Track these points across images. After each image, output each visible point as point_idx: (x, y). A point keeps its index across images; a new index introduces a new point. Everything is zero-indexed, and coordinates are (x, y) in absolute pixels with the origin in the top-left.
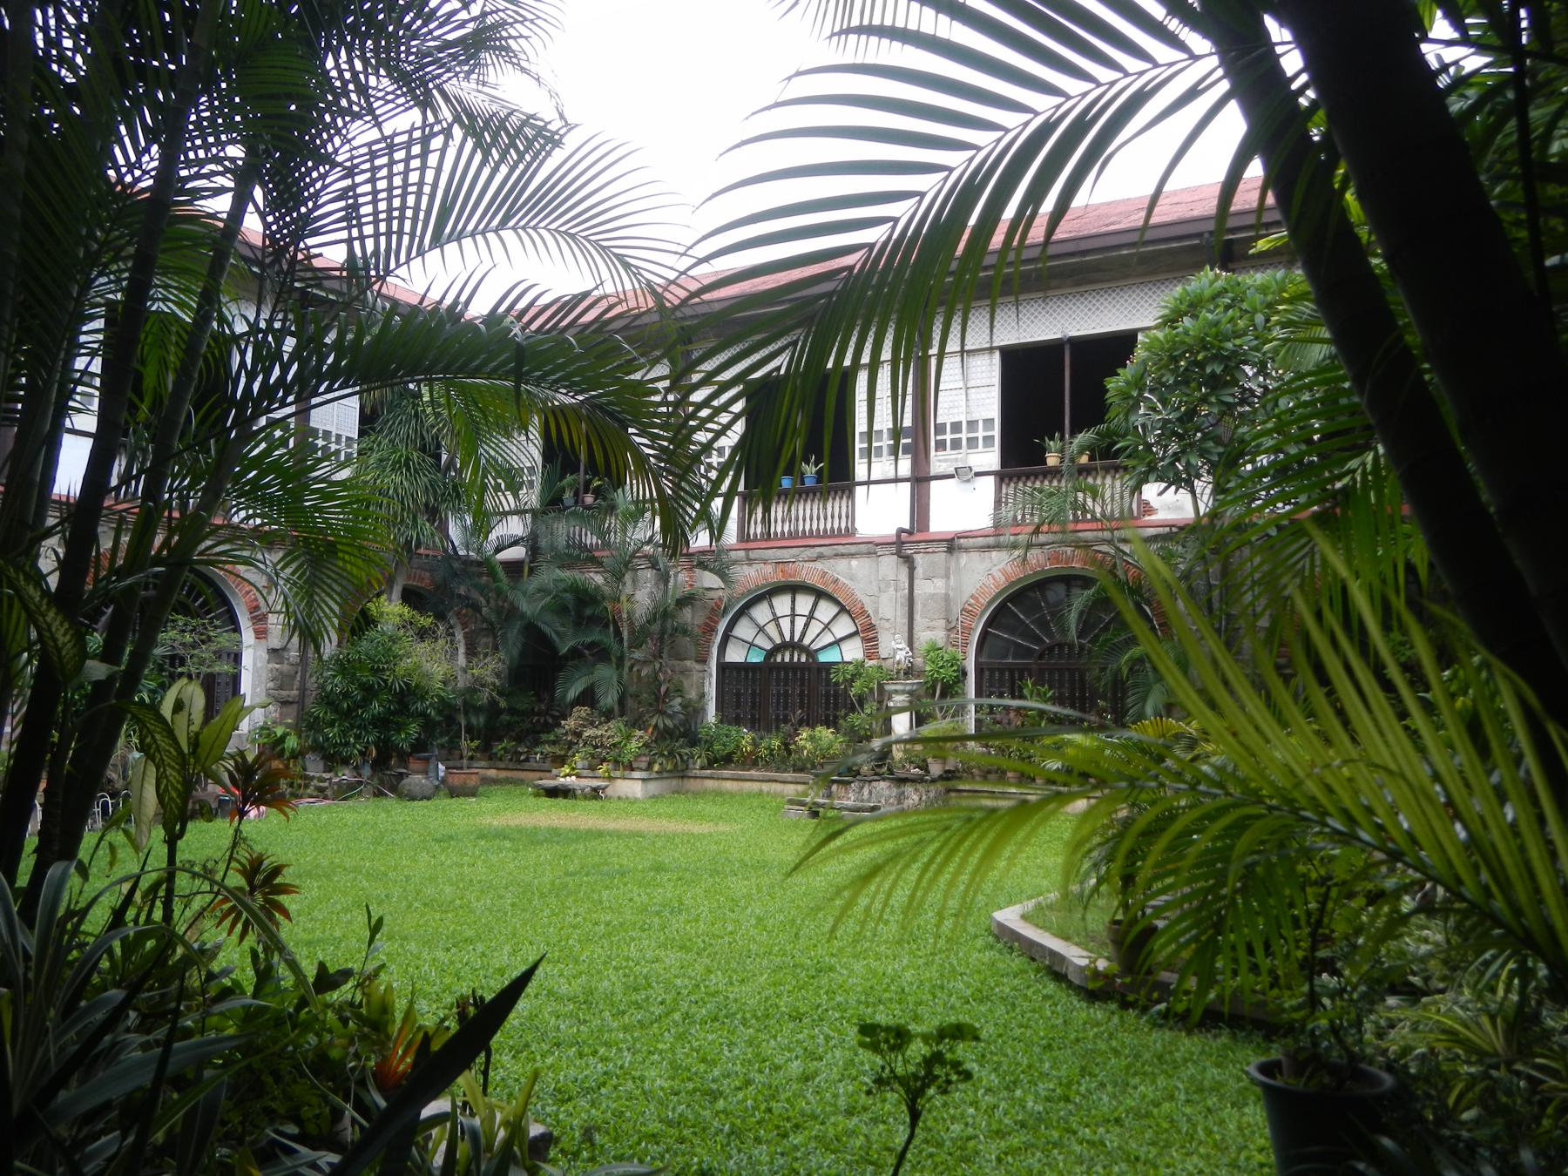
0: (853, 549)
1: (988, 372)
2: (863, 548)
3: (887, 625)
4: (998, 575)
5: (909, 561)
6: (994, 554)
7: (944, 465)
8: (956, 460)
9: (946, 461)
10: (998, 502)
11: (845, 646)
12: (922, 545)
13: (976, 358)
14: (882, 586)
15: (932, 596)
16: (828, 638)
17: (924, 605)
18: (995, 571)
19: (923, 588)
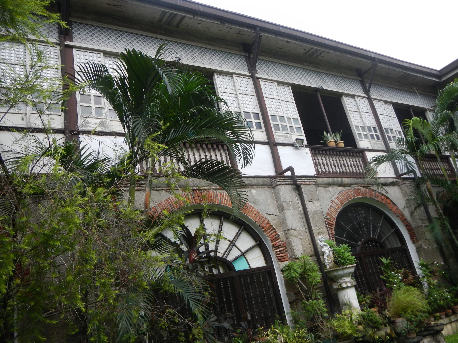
0: (253, 181)
1: (288, 93)
2: (261, 181)
3: (295, 233)
4: (336, 201)
5: (298, 189)
6: (330, 189)
7: (281, 138)
8: (287, 137)
9: (281, 136)
10: (316, 164)
11: (249, 256)
12: (303, 179)
13: (281, 87)
14: (285, 205)
15: (316, 212)
16: (235, 253)
17: (313, 219)
18: (333, 198)
19: (310, 207)
